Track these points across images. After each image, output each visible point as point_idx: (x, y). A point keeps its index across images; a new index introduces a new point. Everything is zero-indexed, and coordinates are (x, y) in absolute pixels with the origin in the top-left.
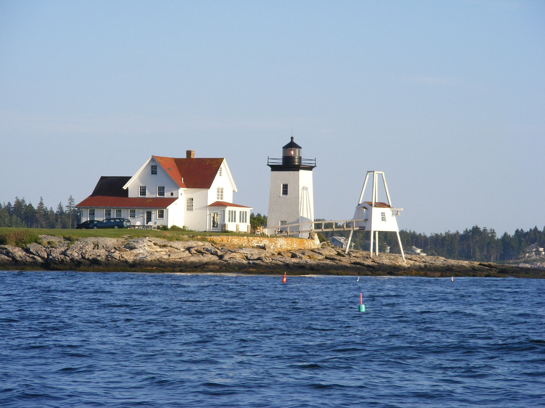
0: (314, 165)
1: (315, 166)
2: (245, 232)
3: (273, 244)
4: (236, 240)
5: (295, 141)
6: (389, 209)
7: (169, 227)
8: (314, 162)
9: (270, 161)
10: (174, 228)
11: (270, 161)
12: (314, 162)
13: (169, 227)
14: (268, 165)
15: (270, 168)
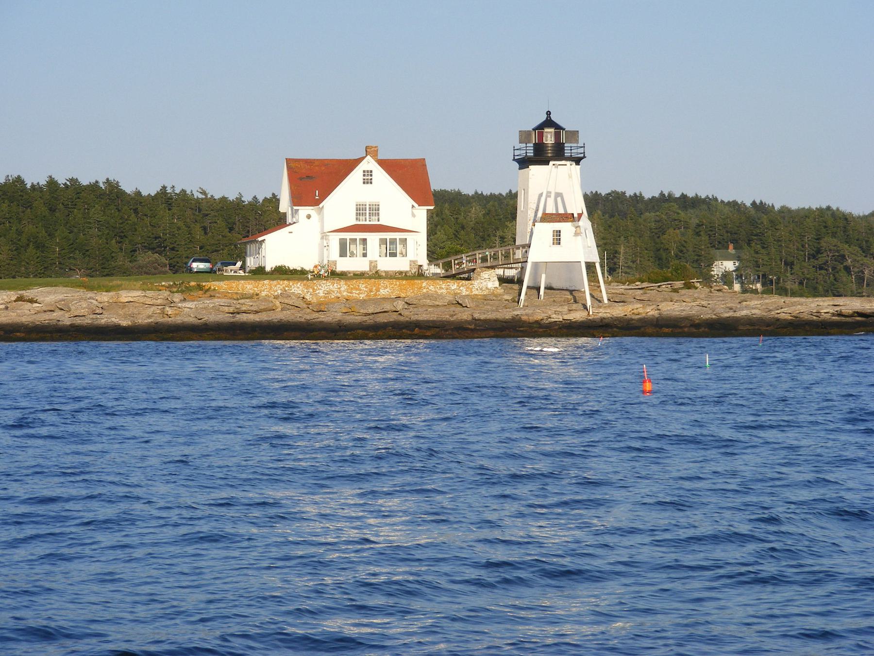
0: (582, 155)
1: (584, 157)
2: (406, 272)
3: (311, 290)
4: (249, 287)
5: (554, 118)
6: (570, 224)
7: (268, 269)
8: (581, 150)
9: (517, 152)
10: (281, 272)
11: (517, 152)
12: (581, 150)
13: (268, 269)
14: (514, 160)
15: (517, 165)
